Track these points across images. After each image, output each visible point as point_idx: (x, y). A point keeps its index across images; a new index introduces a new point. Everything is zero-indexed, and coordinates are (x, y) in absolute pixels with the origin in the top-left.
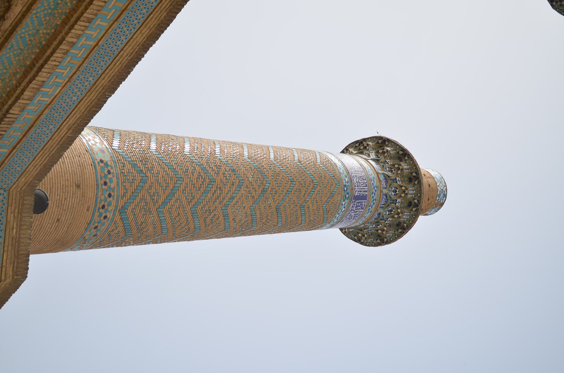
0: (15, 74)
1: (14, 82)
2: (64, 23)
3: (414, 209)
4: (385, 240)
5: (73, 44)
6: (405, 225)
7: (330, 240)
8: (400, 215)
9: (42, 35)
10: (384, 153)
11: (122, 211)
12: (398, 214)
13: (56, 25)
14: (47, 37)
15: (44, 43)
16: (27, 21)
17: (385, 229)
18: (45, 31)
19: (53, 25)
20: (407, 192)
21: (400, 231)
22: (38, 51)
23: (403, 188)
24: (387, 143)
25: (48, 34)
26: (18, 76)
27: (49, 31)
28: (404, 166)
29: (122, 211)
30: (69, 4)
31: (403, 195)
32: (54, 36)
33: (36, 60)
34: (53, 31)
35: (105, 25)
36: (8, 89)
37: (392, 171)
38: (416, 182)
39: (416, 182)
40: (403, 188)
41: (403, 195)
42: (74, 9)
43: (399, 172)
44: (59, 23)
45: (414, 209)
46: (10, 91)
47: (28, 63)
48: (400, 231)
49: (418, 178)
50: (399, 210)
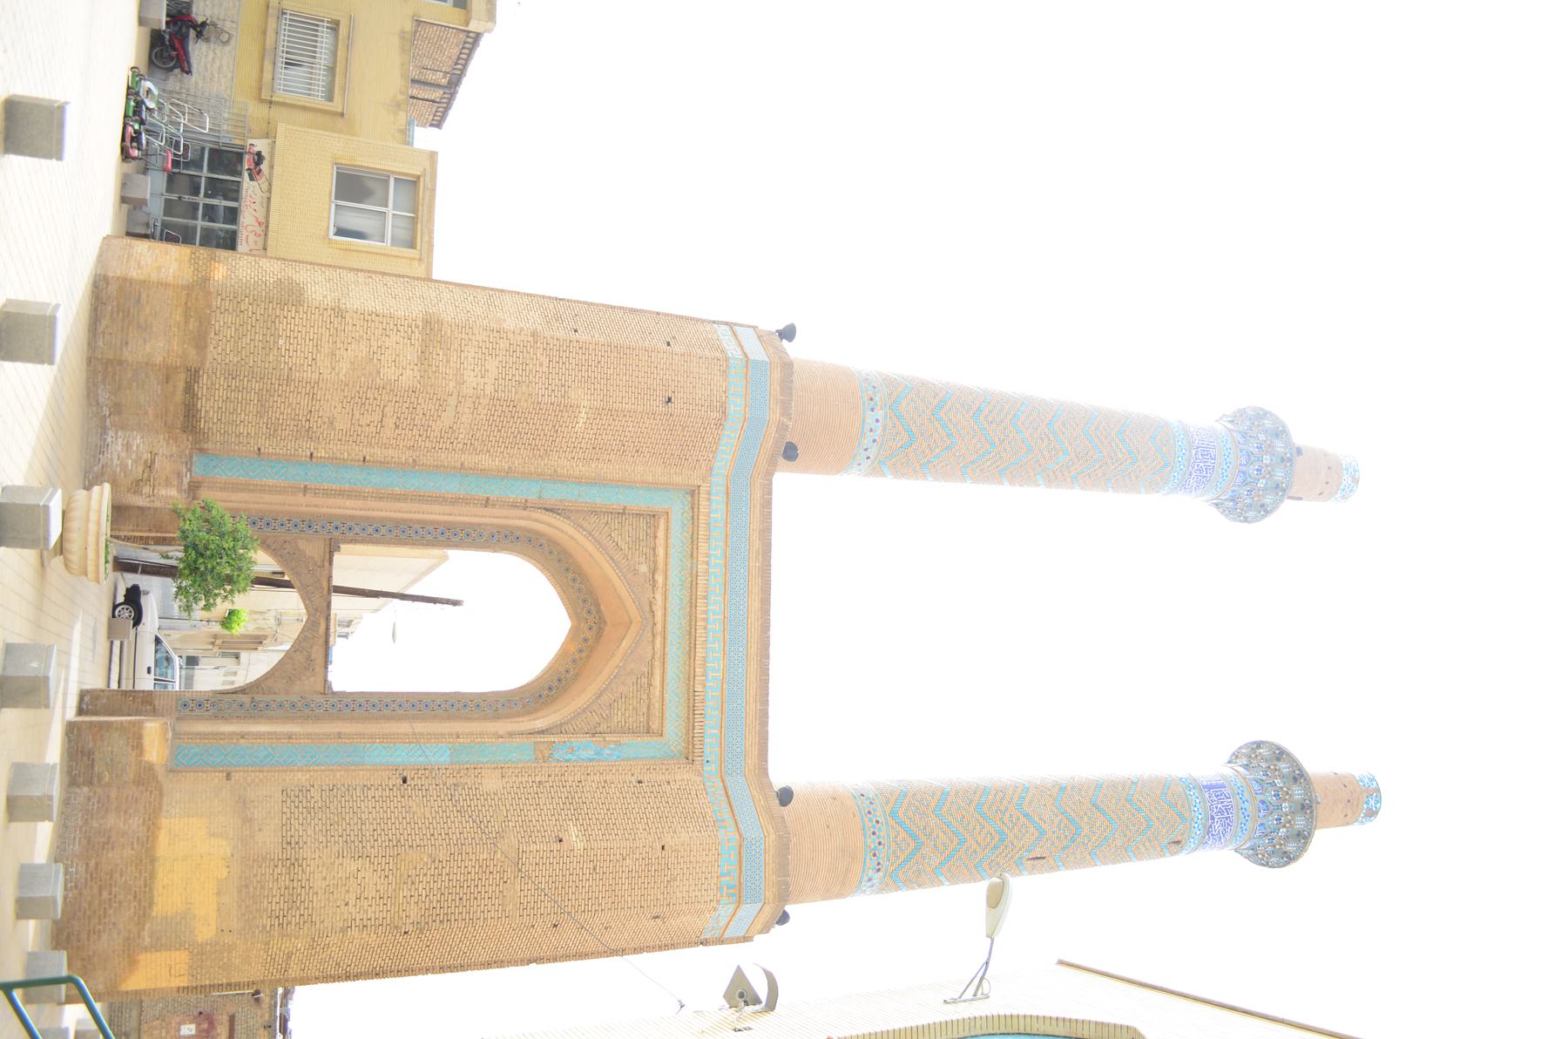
5: (705, 620)
11: (893, 815)
16: (669, 619)
29: (893, 815)
35: (720, 598)
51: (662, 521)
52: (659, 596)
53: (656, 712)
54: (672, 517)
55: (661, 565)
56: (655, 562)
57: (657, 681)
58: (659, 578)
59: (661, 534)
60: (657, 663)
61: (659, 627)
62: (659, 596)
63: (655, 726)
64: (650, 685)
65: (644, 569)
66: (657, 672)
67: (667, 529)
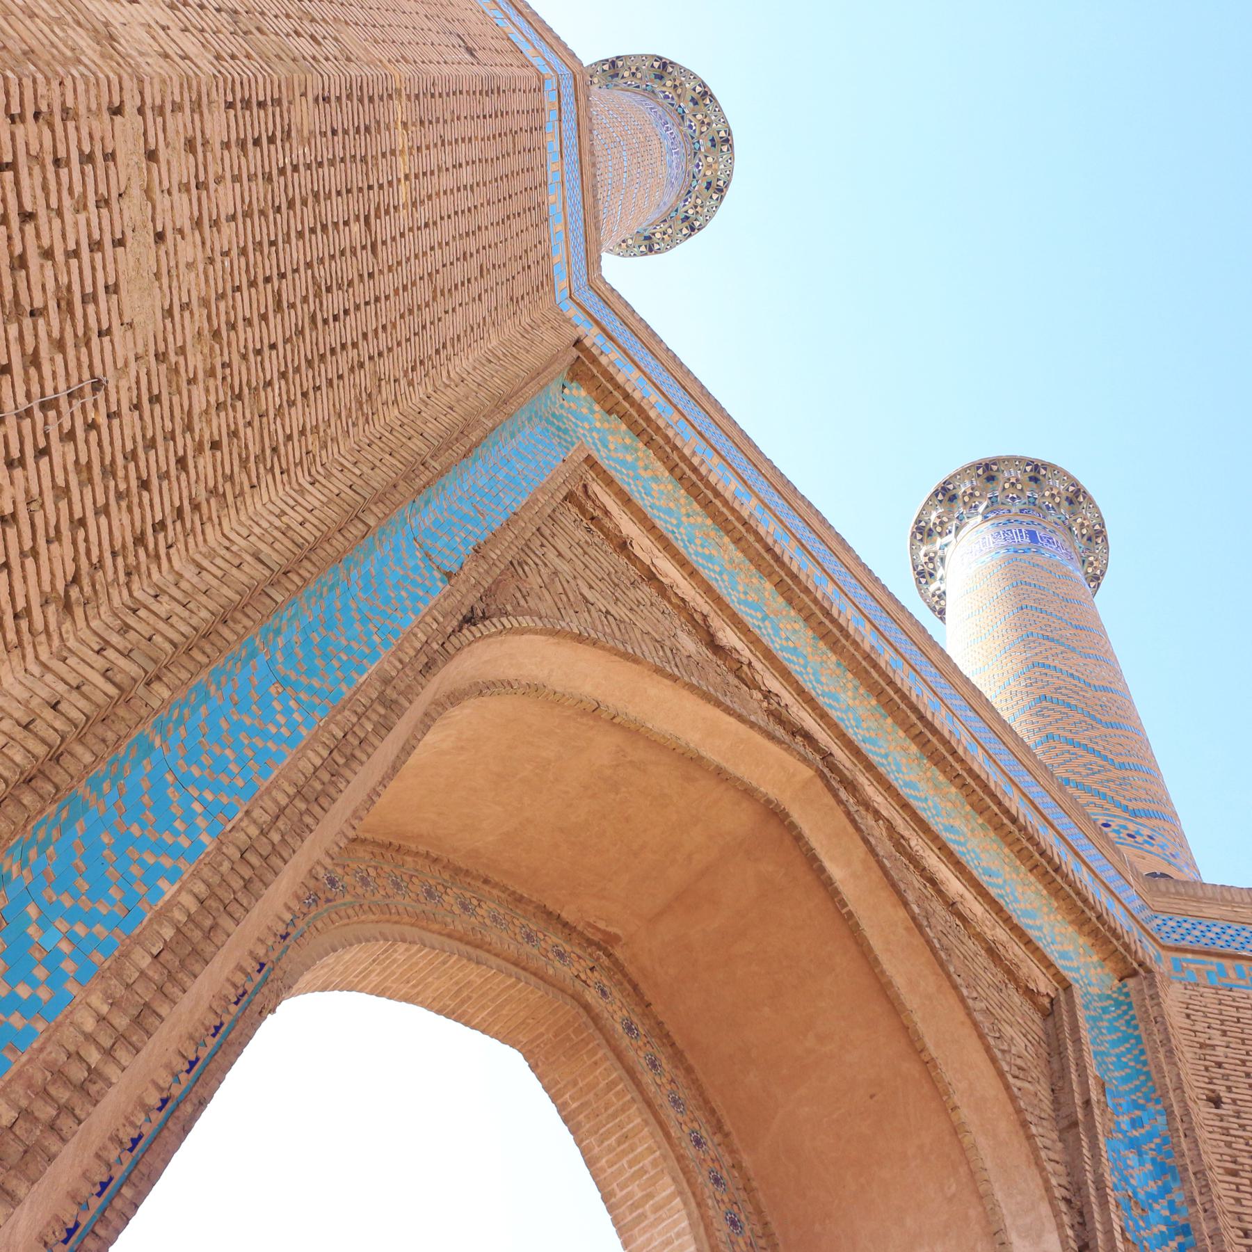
0: (936, 787)
1: (953, 790)
2: (834, 646)
3: (1043, 472)
4: (1097, 527)
6: (1071, 489)
7: (1109, 603)
8: (1055, 492)
9: (857, 702)
10: (942, 523)
12: (1053, 496)
13: (839, 665)
14: (862, 691)
15: (874, 702)
17: (1079, 520)
18: (850, 693)
19: (838, 672)
20: (1013, 480)
21: (1081, 499)
22: (889, 720)
23: (1007, 485)
24: (923, 524)
25: (856, 688)
26: (941, 778)
27: (850, 685)
28: (965, 487)
30: (797, 626)
31: (1019, 486)
32: (860, 674)
33: (908, 728)
34: (850, 676)
36: (968, 808)
37: (976, 507)
38: (995, 468)
39: (995, 468)
40: (1007, 485)
41: (1019, 486)
42: (806, 620)
43: (977, 494)
44: (834, 658)
45: (1043, 472)
46: (972, 805)
47: (914, 749)
48: (1081, 499)
49: (987, 465)
50: (1047, 494)
51: (596, 488)
52: (773, 684)
53: (1015, 951)
54: (595, 455)
55: (700, 603)
56: (683, 606)
57: (954, 886)
58: (728, 637)
59: (629, 527)
60: (917, 843)
61: (841, 756)
62: (773, 684)
63: (1044, 985)
64: (951, 906)
65: (689, 644)
66: (933, 861)
67: (626, 500)
